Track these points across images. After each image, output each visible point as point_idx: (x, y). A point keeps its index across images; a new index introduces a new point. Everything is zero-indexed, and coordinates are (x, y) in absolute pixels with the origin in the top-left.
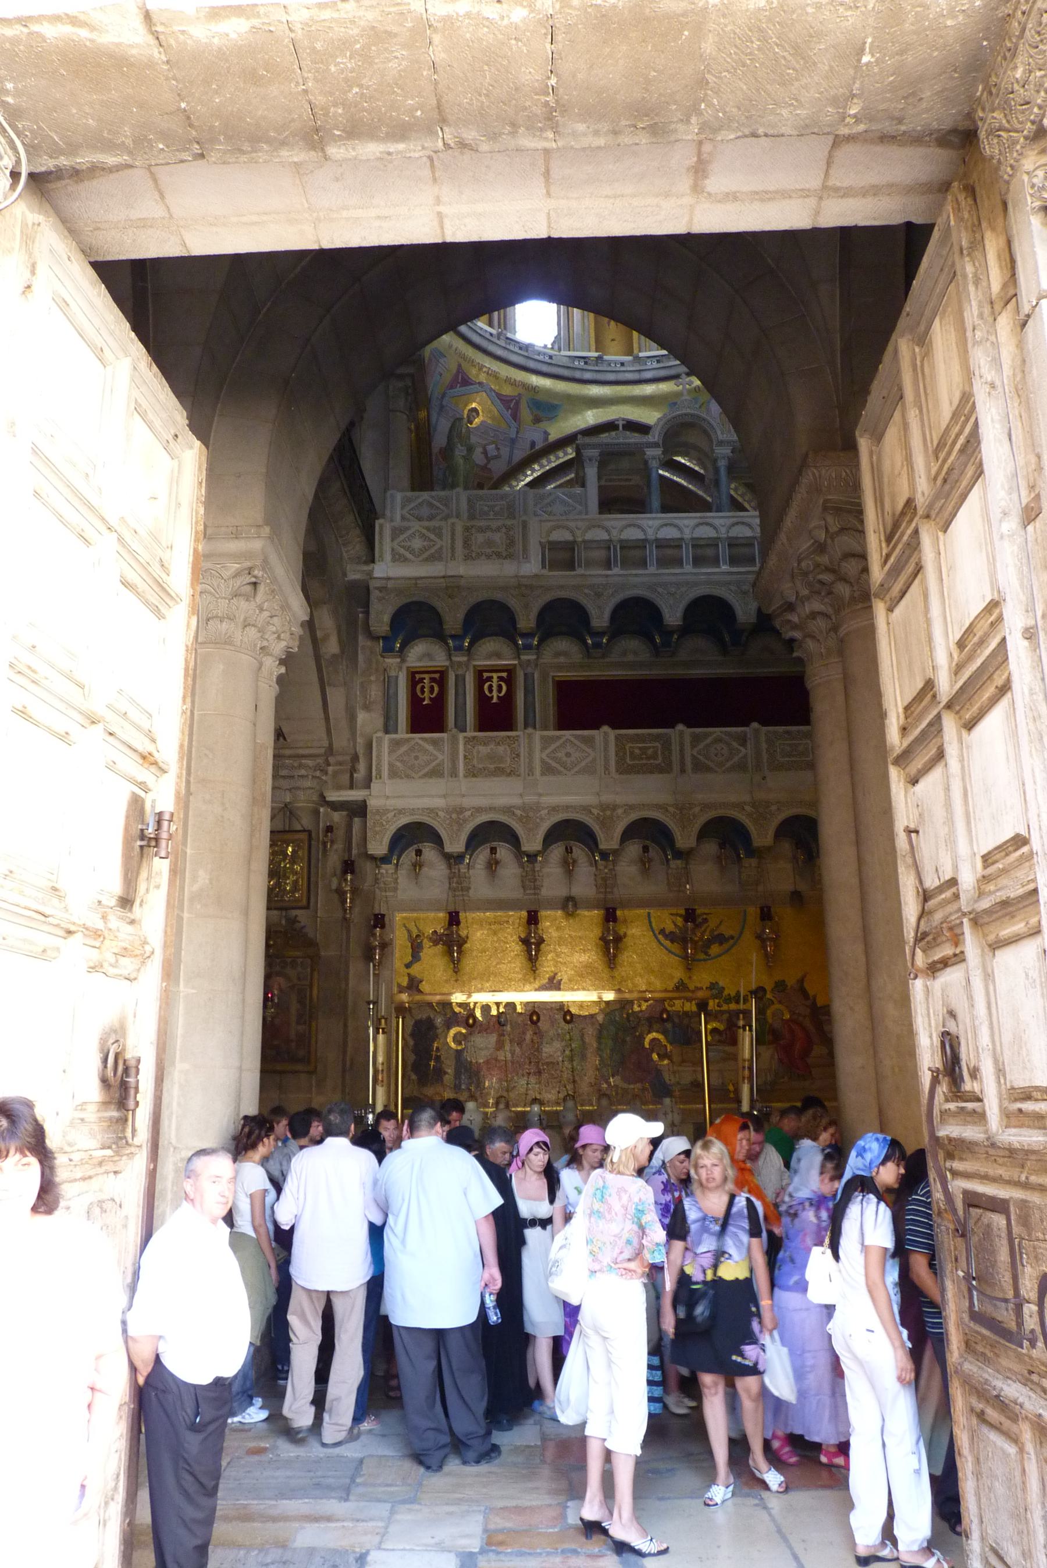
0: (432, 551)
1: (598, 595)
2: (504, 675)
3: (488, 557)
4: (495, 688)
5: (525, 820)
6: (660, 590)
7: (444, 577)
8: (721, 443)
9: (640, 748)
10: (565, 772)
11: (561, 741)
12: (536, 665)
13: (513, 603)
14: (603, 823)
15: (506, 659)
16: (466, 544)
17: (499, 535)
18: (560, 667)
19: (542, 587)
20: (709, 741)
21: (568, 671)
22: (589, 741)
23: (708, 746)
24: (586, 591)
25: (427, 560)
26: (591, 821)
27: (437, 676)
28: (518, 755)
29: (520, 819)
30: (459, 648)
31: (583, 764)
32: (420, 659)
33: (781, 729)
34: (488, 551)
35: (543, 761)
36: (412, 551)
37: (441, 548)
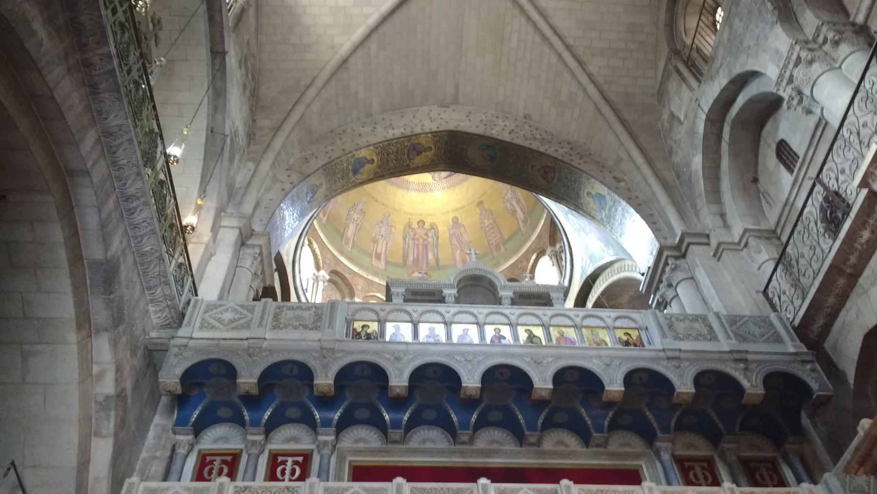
0: (241, 322)
2: (300, 459)
3: (295, 328)
4: (288, 472)
6: (458, 358)
7: (247, 339)
8: (504, 288)
12: (334, 447)
13: (313, 363)
15: (307, 444)
16: (276, 317)
18: (358, 452)
19: (343, 351)
24: (387, 356)
25: (232, 329)
27: (229, 458)
30: (255, 423)
34: (296, 324)
36: (220, 321)
37: (251, 320)
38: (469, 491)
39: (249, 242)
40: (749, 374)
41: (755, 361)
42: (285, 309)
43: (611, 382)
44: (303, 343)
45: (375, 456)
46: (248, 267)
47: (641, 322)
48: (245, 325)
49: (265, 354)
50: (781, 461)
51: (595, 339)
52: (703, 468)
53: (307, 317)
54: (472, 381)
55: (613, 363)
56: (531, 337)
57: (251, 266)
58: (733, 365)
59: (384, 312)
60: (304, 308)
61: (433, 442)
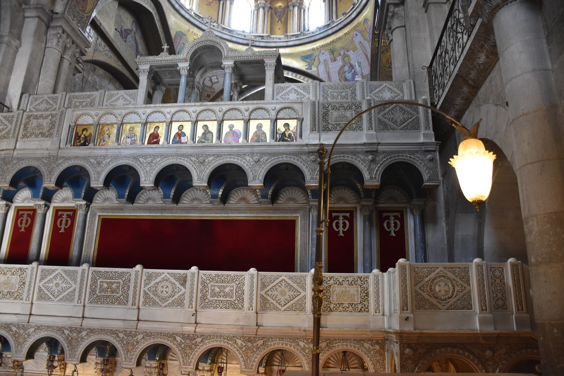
1: (99, 163)
2: (71, 213)
3: (37, 136)
5: (16, 335)
6: (141, 159)
8: (227, 58)
9: (107, 283)
10: (53, 298)
11: (54, 274)
13: (43, 170)
14: (70, 343)
17: (46, 121)
18: (103, 209)
19: (63, 157)
20: (159, 279)
21: (108, 212)
22: (72, 275)
23: (158, 283)
24: (92, 160)
26: (62, 339)
28: (24, 283)
29: (14, 335)
31: (66, 293)
32: (24, 201)
33: (213, 273)
35: (40, 290)
37: (9, 131)
38: (128, 275)
39: (52, 24)
40: (373, 166)
41: (384, 152)
42: (31, 119)
43: (254, 179)
44: (38, 152)
45: (113, 213)
46: (54, 46)
47: (300, 114)
48: (6, 135)
49: (15, 162)
50: (409, 211)
51: (258, 132)
52: (345, 218)
53: (45, 124)
54: (147, 182)
55: (261, 160)
56: (207, 131)
57: (57, 44)
58: (362, 157)
59: (98, 117)
60: (44, 116)
61: (154, 200)
